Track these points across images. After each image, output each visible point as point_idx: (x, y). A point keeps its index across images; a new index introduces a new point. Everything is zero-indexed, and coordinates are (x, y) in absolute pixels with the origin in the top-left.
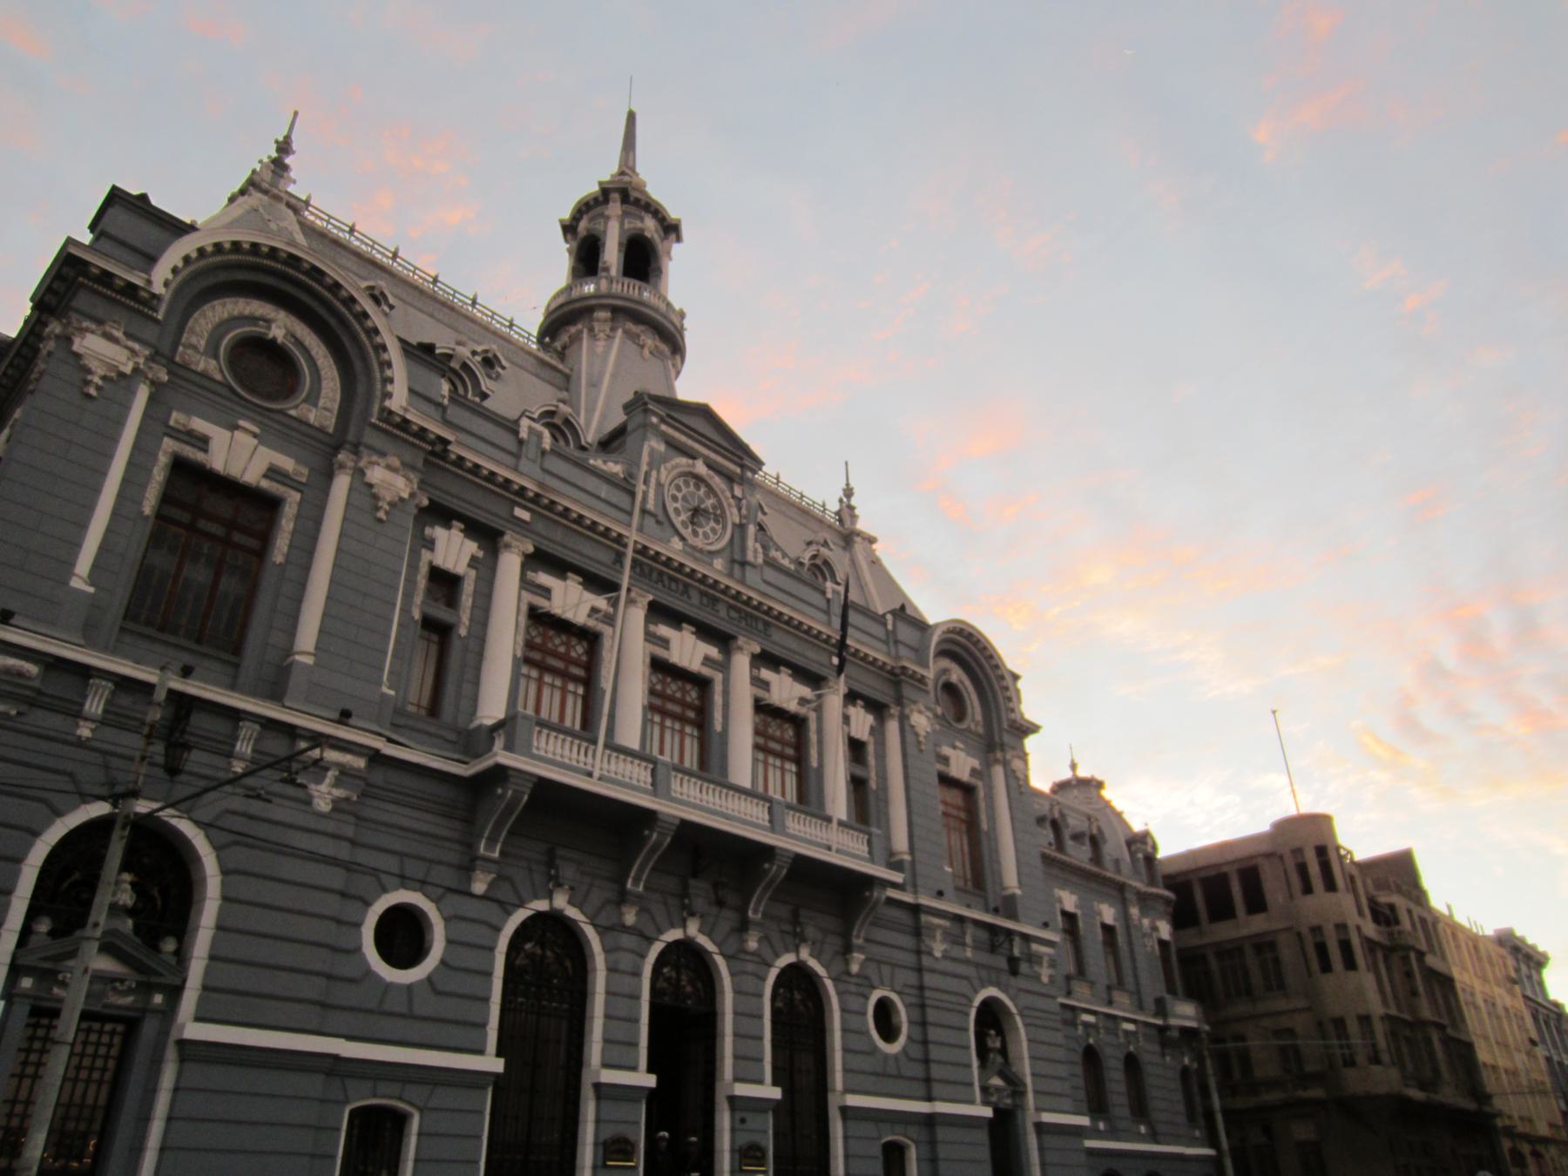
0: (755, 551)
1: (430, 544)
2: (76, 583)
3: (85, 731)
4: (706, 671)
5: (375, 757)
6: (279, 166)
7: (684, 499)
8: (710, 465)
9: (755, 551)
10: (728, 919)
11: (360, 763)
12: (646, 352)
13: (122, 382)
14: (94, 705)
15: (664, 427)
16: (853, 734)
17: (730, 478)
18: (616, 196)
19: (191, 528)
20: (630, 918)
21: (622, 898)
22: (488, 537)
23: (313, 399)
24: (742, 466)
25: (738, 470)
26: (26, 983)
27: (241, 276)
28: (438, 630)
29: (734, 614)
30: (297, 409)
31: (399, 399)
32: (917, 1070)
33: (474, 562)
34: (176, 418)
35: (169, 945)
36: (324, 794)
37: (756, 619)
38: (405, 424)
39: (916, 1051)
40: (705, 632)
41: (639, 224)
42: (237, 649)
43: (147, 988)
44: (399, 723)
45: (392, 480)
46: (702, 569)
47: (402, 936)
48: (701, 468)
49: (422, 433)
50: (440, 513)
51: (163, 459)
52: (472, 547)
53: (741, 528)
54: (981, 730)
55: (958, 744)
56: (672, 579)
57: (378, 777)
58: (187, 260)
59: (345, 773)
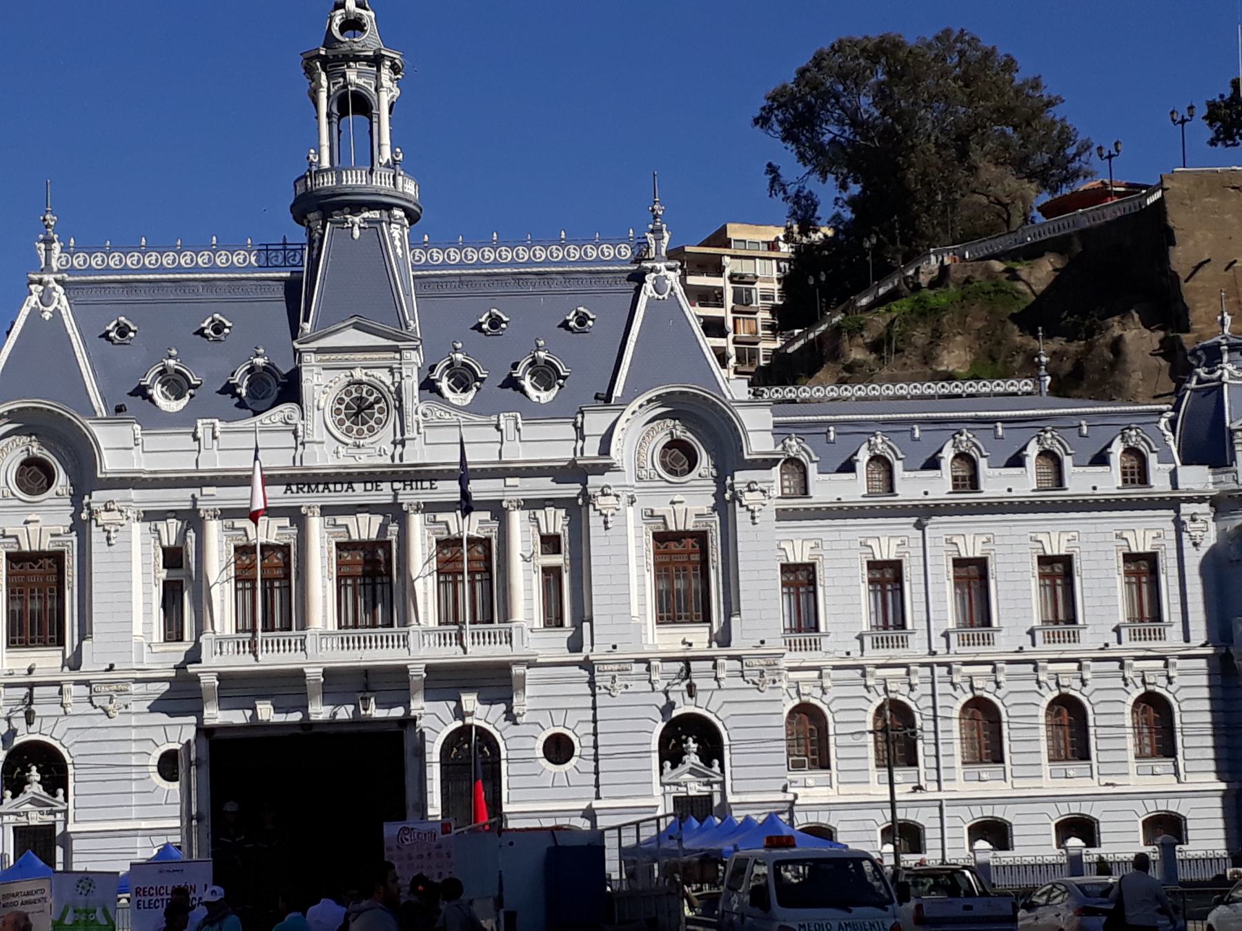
7: (348, 407)
12: (357, 233)
35: (61, 791)
48: (358, 374)
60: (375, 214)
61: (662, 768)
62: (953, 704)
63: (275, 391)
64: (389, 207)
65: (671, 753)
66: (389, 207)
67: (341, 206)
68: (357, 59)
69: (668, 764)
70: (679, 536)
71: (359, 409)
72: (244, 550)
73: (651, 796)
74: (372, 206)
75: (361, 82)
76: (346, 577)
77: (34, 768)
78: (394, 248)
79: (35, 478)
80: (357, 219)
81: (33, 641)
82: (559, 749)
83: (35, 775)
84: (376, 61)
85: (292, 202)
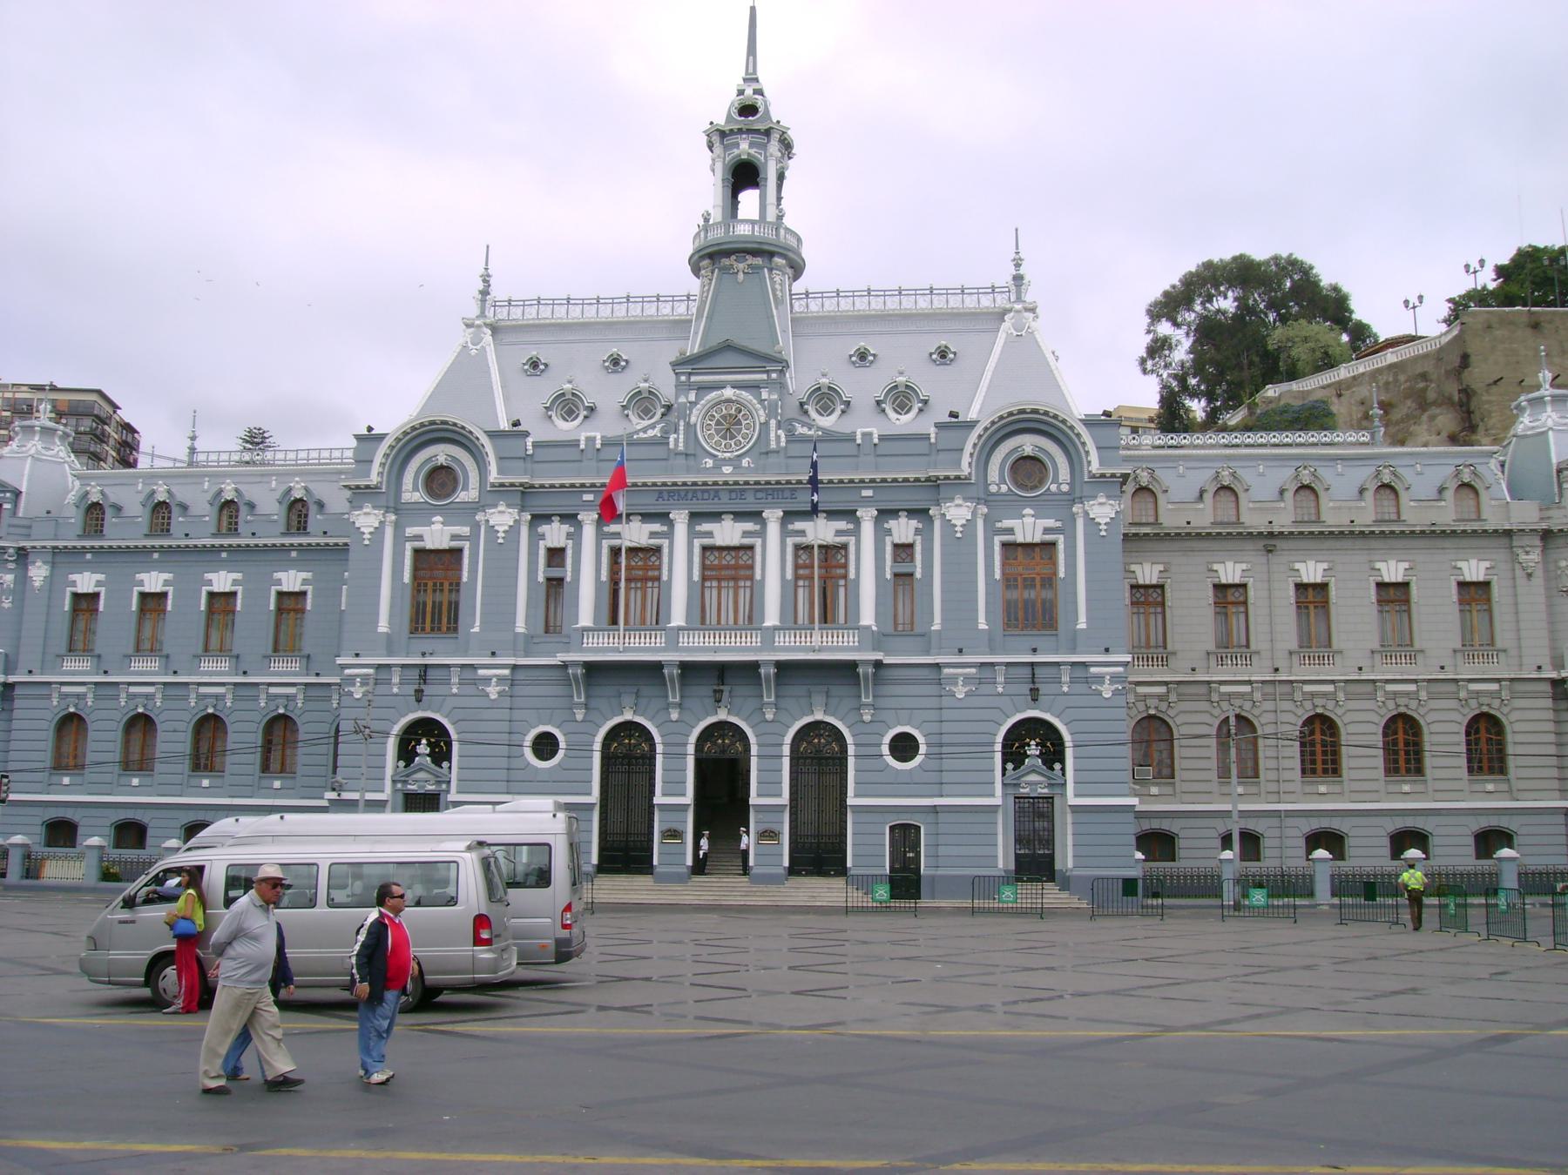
0: (778, 437)
1: (542, 537)
2: (381, 630)
3: (395, 690)
4: (747, 541)
5: (515, 667)
6: (485, 293)
7: (718, 423)
8: (736, 386)
9: (778, 437)
10: (751, 704)
11: (506, 672)
12: (741, 276)
13: (379, 531)
14: (396, 680)
15: (693, 379)
16: (897, 541)
17: (754, 387)
18: (716, 139)
19: (431, 578)
20: (674, 715)
21: (668, 706)
22: (570, 518)
23: (465, 488)
24: (767, 372)
25: (764, 376)
26: (399, 786)
27: (415, 443)
28: (555, 585)
29: (759, 495)
30: (462, 496)
31: (494, 476)
32: (933, 777)
33: (569, 536)
34: (410, 531)
36: (493, 691)
37: (783, 490)
38: (502, 485)
39: (934, 764)
40: (739, 516)
41: (736, 152)
42: (456, 630)
43: (439, 783)
44: (529, 644)
45: (502, 517)
46: (720, 479)
47: (546, 746)
48: (729, 393)
49: (512, 485)
50: (539, 518)
51: (408, 554)
52: (566, 528)
53: (765, 425)
54: (1065, 488)
55: (1028, 511)
56: (703, 491)
57: (520, 675)
58: (386, 456)
59: (501, 679)
60: (758, 261)
61: (1004, 770)
62: (1292, 719)
63: (660, 411)
64: (771, 254)
65: (1013, 753)
66: (771, 254)
67: (727, 253)
68: (749, 131)
69: (1010, 766)
70: (1028, 546)
71: (730, 425)
72: (615, 552)
73: (993, 795)
74: (755, 253)
75: (752, 151)
76: (711, 579)
77: (424, 741)
78: (774, 290)
79: (443, 485)
80: (741, 266)
81: (432, 629)
82: (904, 747)
83: (423, 748)
84: (767, 133)
85: (691, 252)
